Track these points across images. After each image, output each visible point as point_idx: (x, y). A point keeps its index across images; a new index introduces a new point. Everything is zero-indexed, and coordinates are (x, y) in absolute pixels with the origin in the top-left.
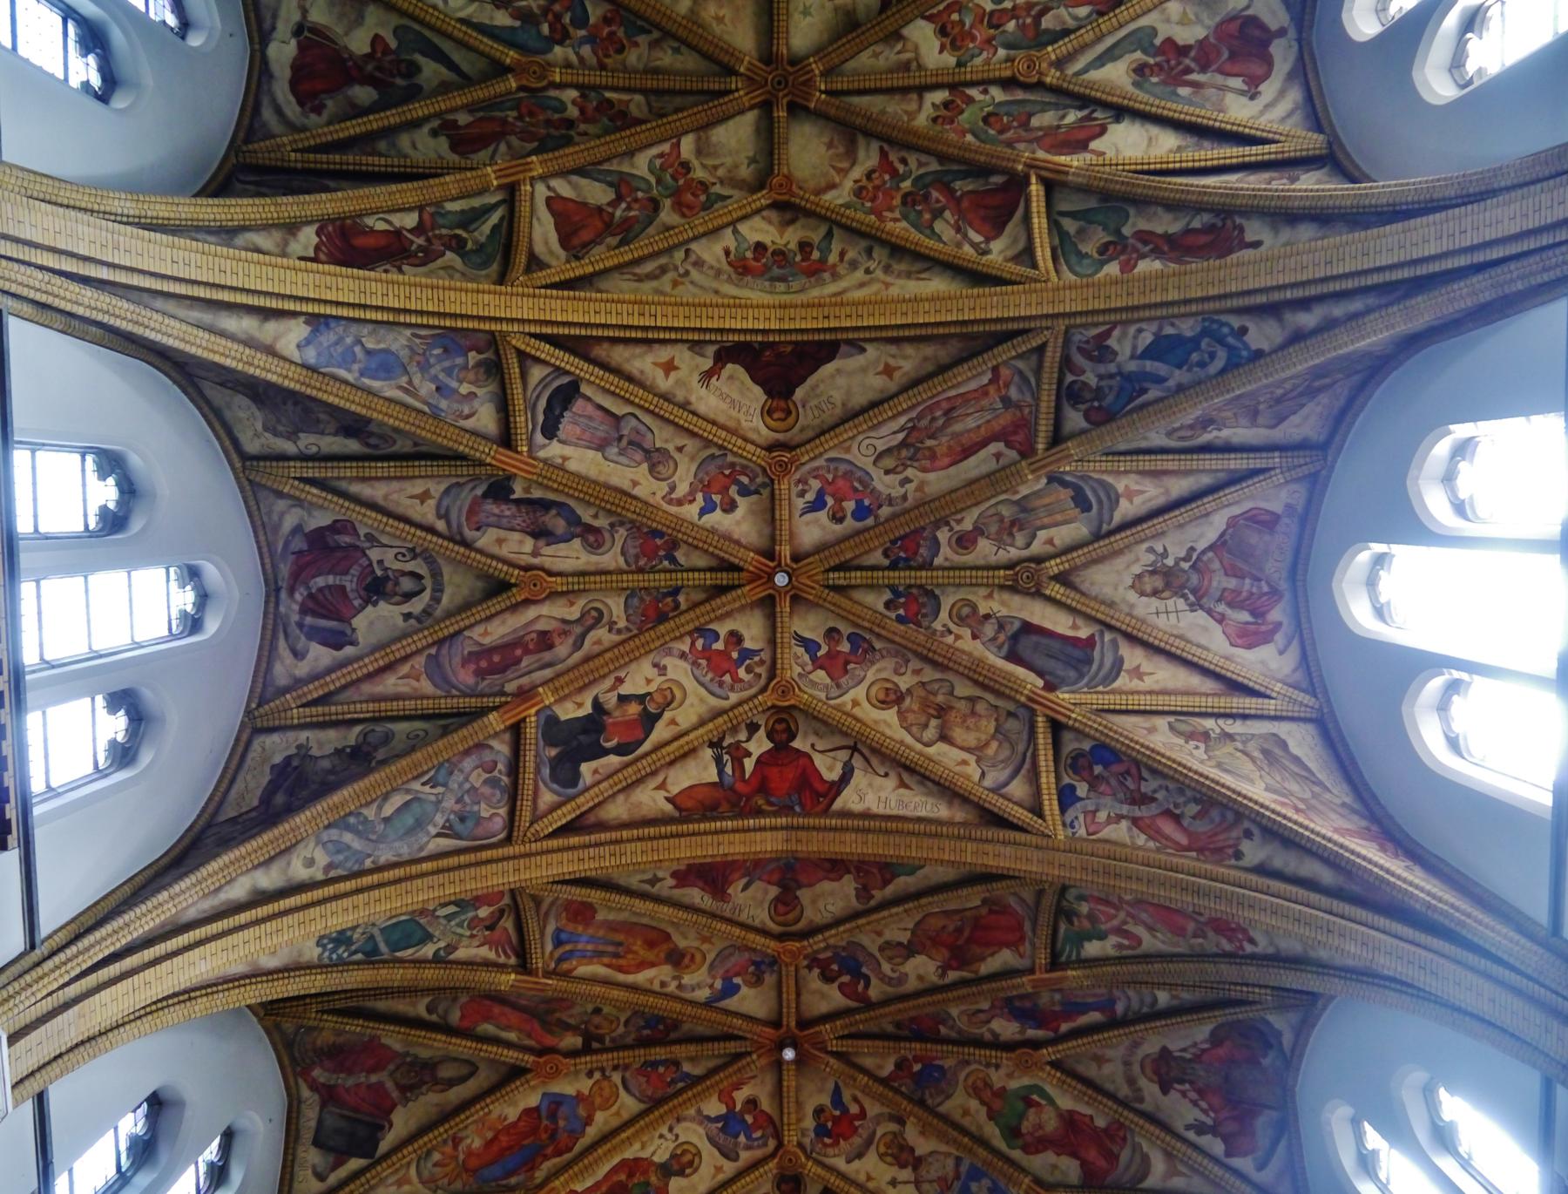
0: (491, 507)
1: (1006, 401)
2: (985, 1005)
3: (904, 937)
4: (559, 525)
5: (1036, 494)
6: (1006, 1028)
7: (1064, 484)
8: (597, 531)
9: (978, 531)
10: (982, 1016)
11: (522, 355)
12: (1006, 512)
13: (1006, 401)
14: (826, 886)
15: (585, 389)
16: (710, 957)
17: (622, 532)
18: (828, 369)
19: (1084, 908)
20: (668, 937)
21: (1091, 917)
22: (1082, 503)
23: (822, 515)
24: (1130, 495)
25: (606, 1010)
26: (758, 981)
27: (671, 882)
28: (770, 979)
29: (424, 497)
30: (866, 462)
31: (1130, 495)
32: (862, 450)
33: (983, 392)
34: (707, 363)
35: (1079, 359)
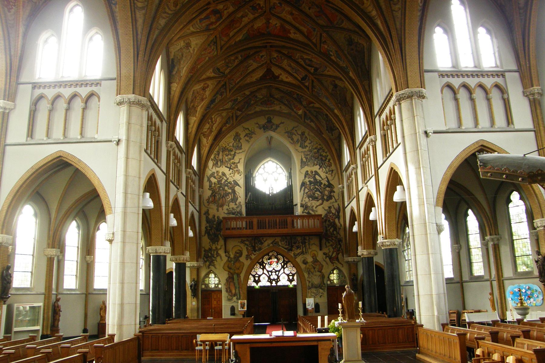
0: (317, 66)
1: (233, 80)
2: (225, 12)
3: (244, 19)
4: (307, 61)
5: (226, 69)
6: (220, 7)
7: (222, 73)
8: (301, 59)
9: (234, 60)
10: (225, 8)
11: (308, 89)
12: (230, 65)
13: (233, 80)
14: (260, 25)
15: (300, 79)
16: (284, 12)
17: (297, 57)
18: (261, 75)
19: (212, 48)
20: (293, 18)
21: (211, 47)
22: (218, 69)
23: (261, 55)
24: (211, 73)
25: (307, 8)
26: (274, 3)
27: (291, 31)
28: (272, 4)
29: (328, 71)
30: (254, 63)
31: (211, 73)
32: (255, 65)
33: (237, 80)
34: (281, 76)
35: (224, 91)
